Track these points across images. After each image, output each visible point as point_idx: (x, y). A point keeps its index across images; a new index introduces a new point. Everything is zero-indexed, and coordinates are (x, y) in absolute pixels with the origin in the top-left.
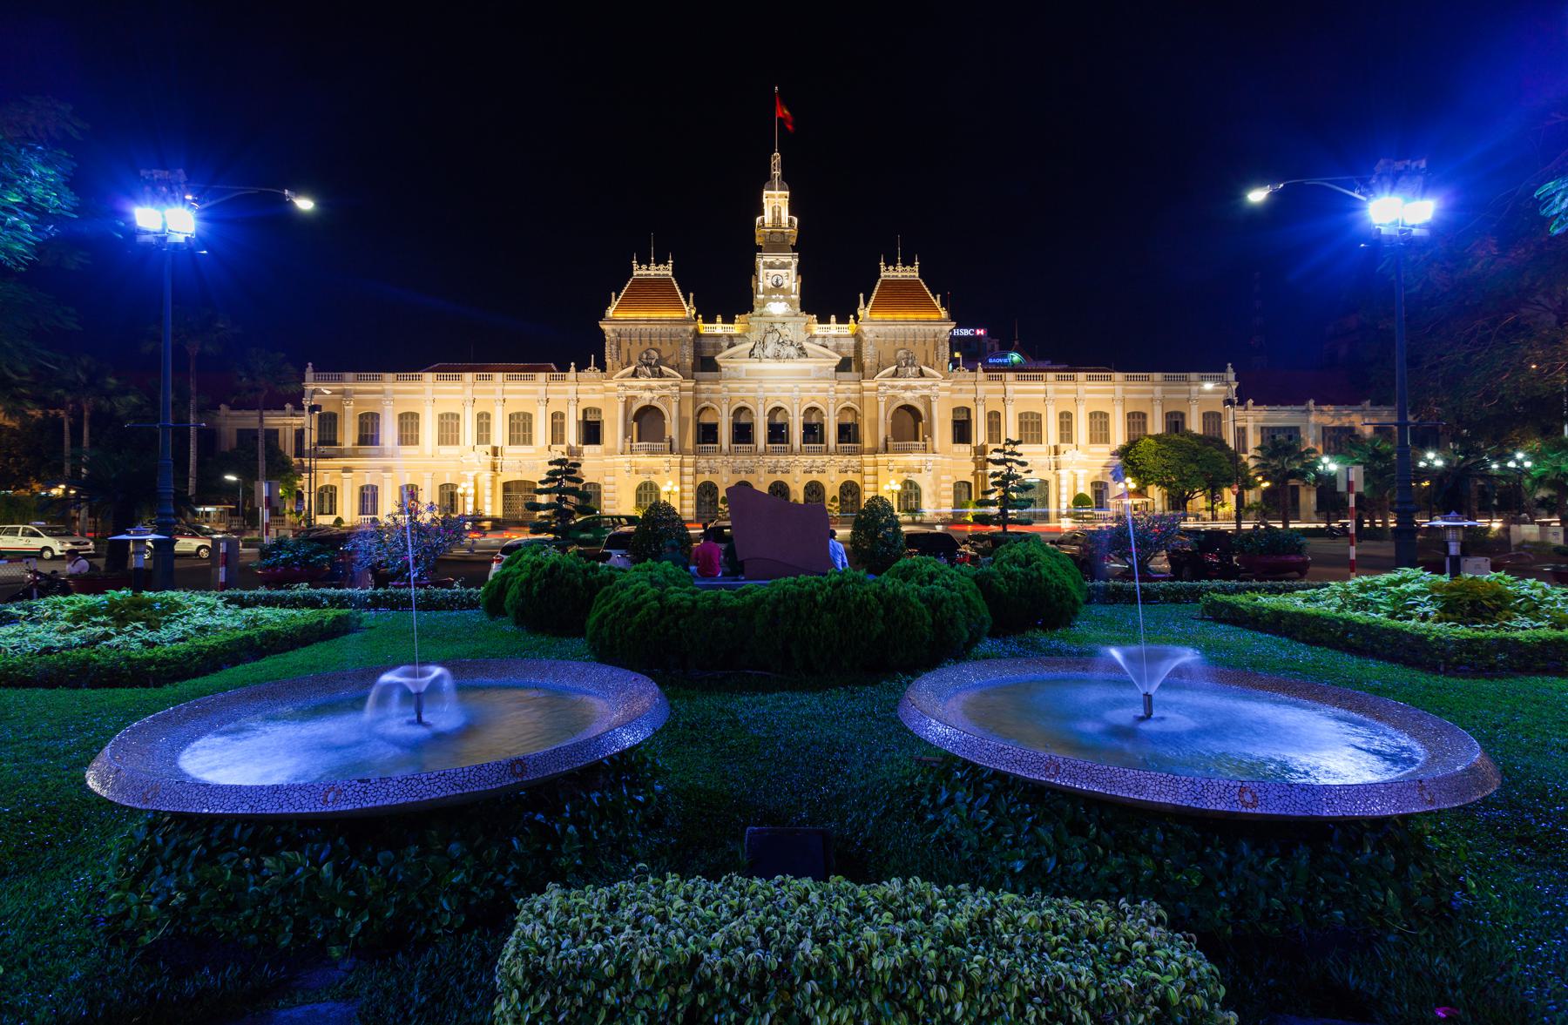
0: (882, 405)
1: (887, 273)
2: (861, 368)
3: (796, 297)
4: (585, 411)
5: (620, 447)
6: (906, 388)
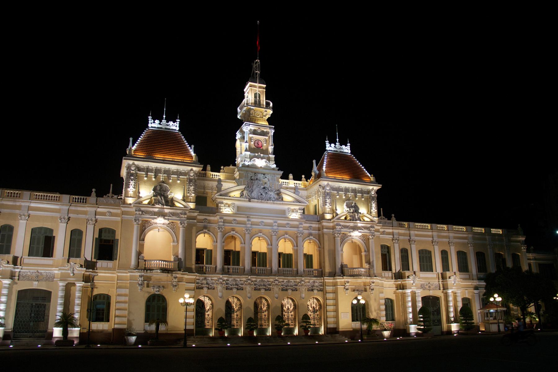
4: (101, 231)
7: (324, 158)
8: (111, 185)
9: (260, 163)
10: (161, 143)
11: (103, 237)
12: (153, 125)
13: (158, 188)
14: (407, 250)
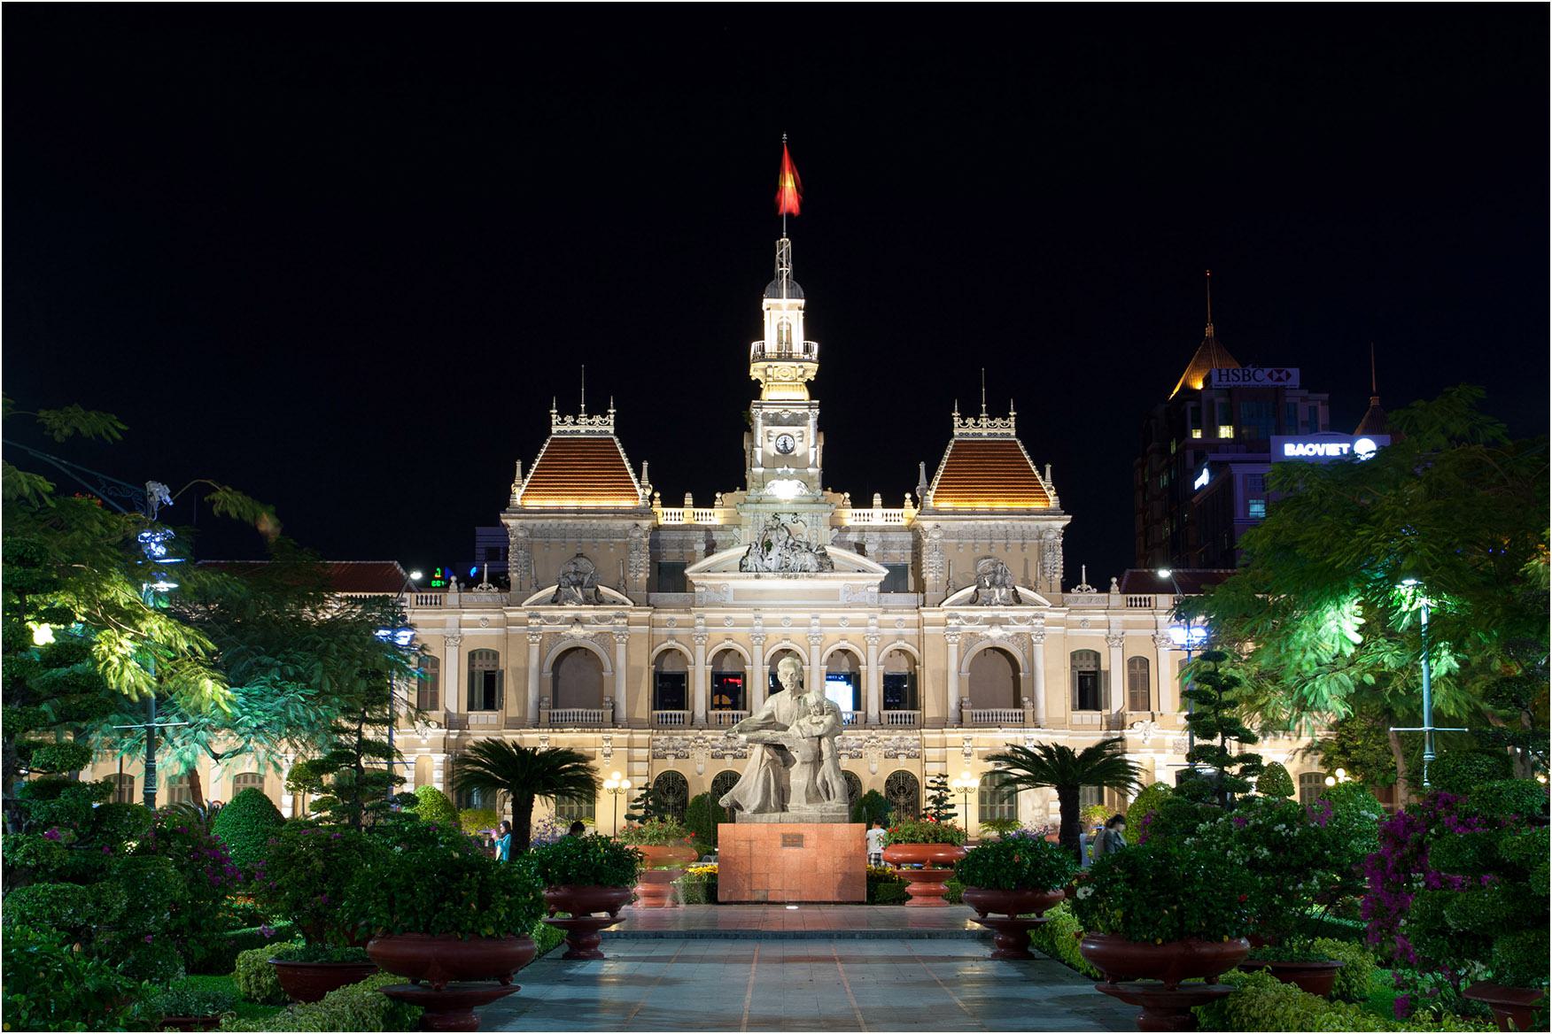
0: (953, 649)
1: (965, 429)
2: (920, 587)
3: (815, 471)
4: (472, 655)
5: (531, 715)
6: (992, 622)
12: (562, 428)
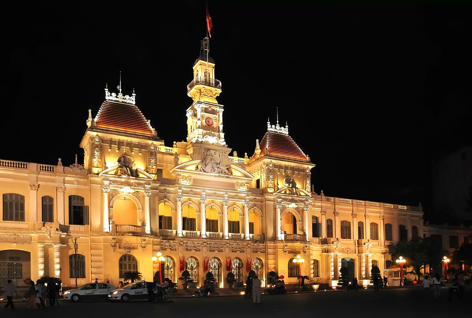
4: (70, 197)
7: (266, 139)
8: (76, 155)
9: (211, 140)
10: (118, 115)
11: (73, 204)
13: (122, 159)
14: (332, 221)
